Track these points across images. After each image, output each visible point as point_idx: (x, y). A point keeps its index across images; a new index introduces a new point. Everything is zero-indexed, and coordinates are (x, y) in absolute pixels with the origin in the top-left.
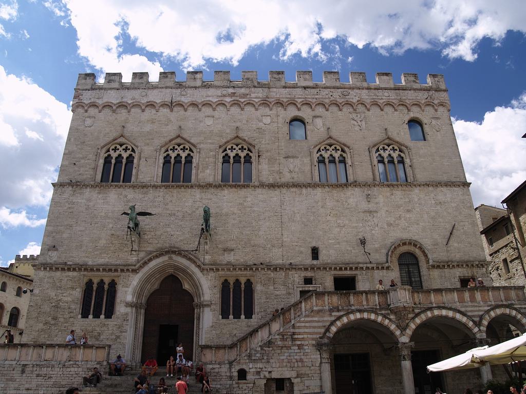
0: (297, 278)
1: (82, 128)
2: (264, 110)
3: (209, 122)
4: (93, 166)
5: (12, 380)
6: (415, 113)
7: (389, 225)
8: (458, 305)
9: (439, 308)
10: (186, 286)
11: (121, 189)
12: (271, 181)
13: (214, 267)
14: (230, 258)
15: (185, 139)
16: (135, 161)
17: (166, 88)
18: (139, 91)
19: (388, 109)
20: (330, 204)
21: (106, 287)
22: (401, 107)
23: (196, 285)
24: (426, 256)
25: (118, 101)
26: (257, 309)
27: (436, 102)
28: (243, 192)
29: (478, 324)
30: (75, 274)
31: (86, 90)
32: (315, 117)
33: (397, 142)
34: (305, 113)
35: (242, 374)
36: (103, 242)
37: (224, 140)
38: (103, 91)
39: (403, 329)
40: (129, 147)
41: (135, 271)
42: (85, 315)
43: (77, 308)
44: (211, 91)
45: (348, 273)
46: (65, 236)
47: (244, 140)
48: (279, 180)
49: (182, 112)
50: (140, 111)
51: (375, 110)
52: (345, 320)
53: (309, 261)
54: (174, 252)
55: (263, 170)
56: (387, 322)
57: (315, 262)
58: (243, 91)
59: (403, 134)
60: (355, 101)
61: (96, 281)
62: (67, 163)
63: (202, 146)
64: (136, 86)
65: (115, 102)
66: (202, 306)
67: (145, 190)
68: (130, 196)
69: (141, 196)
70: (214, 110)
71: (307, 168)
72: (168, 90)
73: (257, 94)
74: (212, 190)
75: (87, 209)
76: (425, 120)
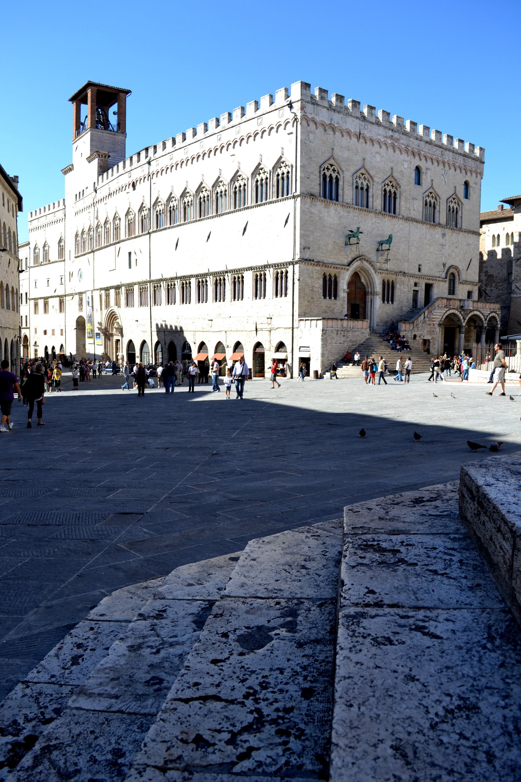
0: (412, 281)
1: (308, 142)
2: (404, 156)
3: (378, 158)
4: (318, 182)
5: (333, 338)
6: (468, 178)
7: (449, 255)
8: (481, 310)
9: (476, 310)
10: (363, 280)
11: (336, 206)
12: (405, 215)
13: (381, 271)
14: (389, 266)
15: (367, 172)
16: (341, 183)
17: (357, 118)
18: (341, 115)
19: (458, 170)
20: (428, 237)
21: (333, 278)
22: (463, 171)
23: (372, 283)
24: (459, 275)
25: (329, 122)
26: (396, 298)
27: (479, 171)
28: (395, 220)
29: (486, 320)
30: (318, 268)
31: (308, 102)
32: (427, 169)
33: (459, 199)
34: (423, 165)
35: (415, 336)
36: (330, 247)
37: (386, 177)
38: (318, 107)
39: (464, 320)
40: (336, 169)
41: (348, 270)
42: (325, 297)
43: (321, 291)
44: (381, 130)
45: (430, 282)
46: (311, 239)
47: (395, 180)
48: (409, 216)
49: (364, 144)
50: (340, 136)
51: (453, 169)
52: (448, 313)
53: (417, 272)
54: (365, 260)
55: (402, 205)
56: (460, 315)
57: (419, 274)
58: (396, 135)
59: (461, 193)
60: (446, 161)
61: (328, 274)
62: (303, 176)
63: (375, 179)
64: (339, 109)
65: (328, 122)
66: (373, 293)
67: (348, 209)
68: (341, 213)
69: (347, 214)
70: (381, 147)
71: (421, 209)
72: (357, 121)
73: (404, 140)
74: (380, 216)
75: (320, 219)
76: (471, 184)
